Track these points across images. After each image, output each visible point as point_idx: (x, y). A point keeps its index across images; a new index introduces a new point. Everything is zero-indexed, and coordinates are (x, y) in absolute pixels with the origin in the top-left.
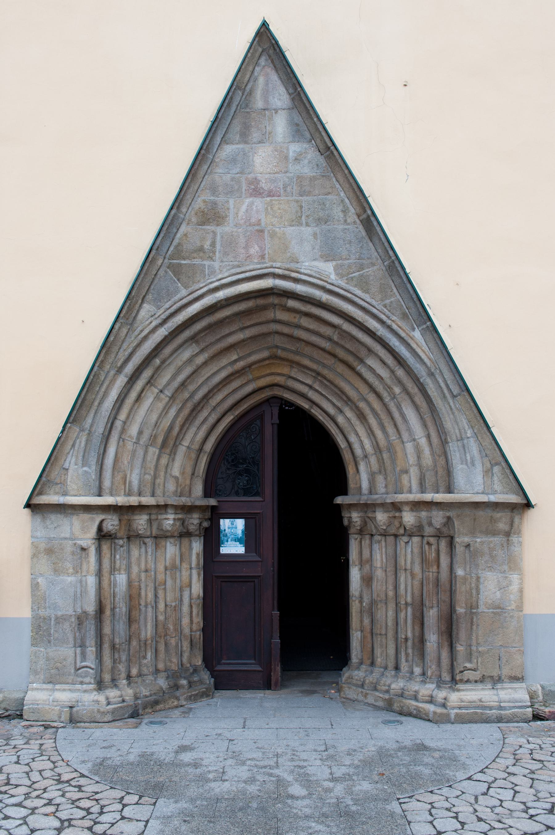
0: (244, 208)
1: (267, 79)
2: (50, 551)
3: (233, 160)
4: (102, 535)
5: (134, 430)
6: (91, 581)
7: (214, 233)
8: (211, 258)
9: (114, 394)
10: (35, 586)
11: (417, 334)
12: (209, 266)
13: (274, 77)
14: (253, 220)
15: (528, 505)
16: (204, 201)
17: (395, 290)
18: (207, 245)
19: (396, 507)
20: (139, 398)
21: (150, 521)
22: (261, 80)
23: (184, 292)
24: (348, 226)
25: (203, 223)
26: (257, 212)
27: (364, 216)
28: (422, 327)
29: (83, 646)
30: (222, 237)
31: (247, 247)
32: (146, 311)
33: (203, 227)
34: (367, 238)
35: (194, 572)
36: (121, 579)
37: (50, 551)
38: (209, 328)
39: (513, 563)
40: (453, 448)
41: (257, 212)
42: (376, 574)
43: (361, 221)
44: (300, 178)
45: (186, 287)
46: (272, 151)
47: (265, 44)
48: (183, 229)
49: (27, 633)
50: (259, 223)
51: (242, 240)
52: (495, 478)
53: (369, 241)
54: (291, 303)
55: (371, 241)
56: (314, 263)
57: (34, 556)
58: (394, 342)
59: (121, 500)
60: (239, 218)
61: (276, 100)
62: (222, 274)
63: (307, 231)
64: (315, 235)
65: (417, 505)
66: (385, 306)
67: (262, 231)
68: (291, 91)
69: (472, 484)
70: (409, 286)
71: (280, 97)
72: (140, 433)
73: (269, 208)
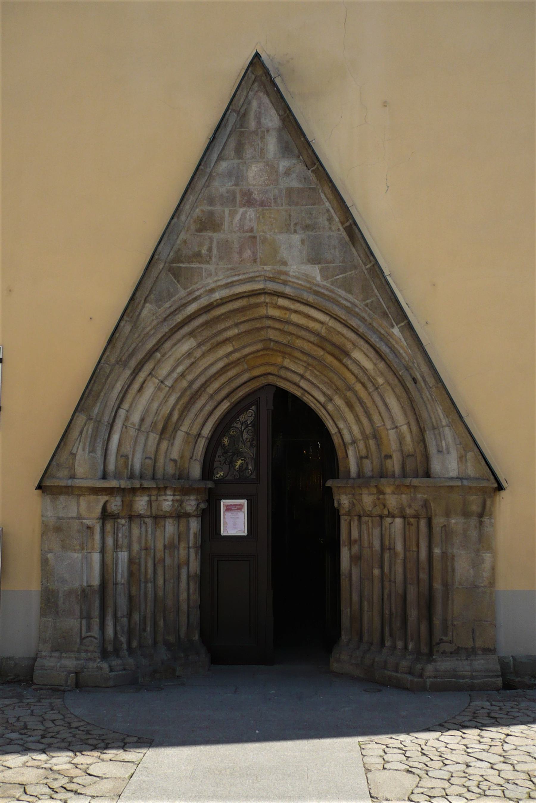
0: (238, 217)
2: (58, 529)
3: (230, 174)
4: (106, 515)
5: (136, 418)
6: (96, 557)
7: (211, 239)
8: (208, 262)
9: (119, 386)
10: (44, 562)
11: (396, 331)
12: (206, 269)
13: (266, 100)
14: (246, 228)
15: (500, 488)
16: (202, 211)
17: (376, 291)
18: (204, 251)
20: (141, 389)
21: (150, 502)
22: (255, 104)
23: (182, 293)
25: (199, 230)
26: (250, 220)
27: (348, 224)
28: (400, 325)
29: (89, 618)
30: (218, 243)
31: (240, 253)
33: (201, 234)
34: (350, 243)
35: (192, 551)
36: (123, 556)
37: (58, 529)
38: (206, 324)
40: (429, 436)
41: (250, 220)
43: (344, 228)
44: (290, 191)
45: (185, 289)
48: (183, 236)
50: (251, 230)
51: (236, 246)
52: (469, 464)
53: (352, 246)
54: (282, 302)
55: (354, 246)
57: (43, 534)
58: (374, 339)
59: (123, 484)
60: (234, 226)
61: (267, 120)
63: (296, 238)
64: (303, 241)
66: (367, 305)
67: (255, 237)
68: (281, 112)
70: (387, 287)
71: (272, 120)
72: (142, 420)
73: (261, 217)
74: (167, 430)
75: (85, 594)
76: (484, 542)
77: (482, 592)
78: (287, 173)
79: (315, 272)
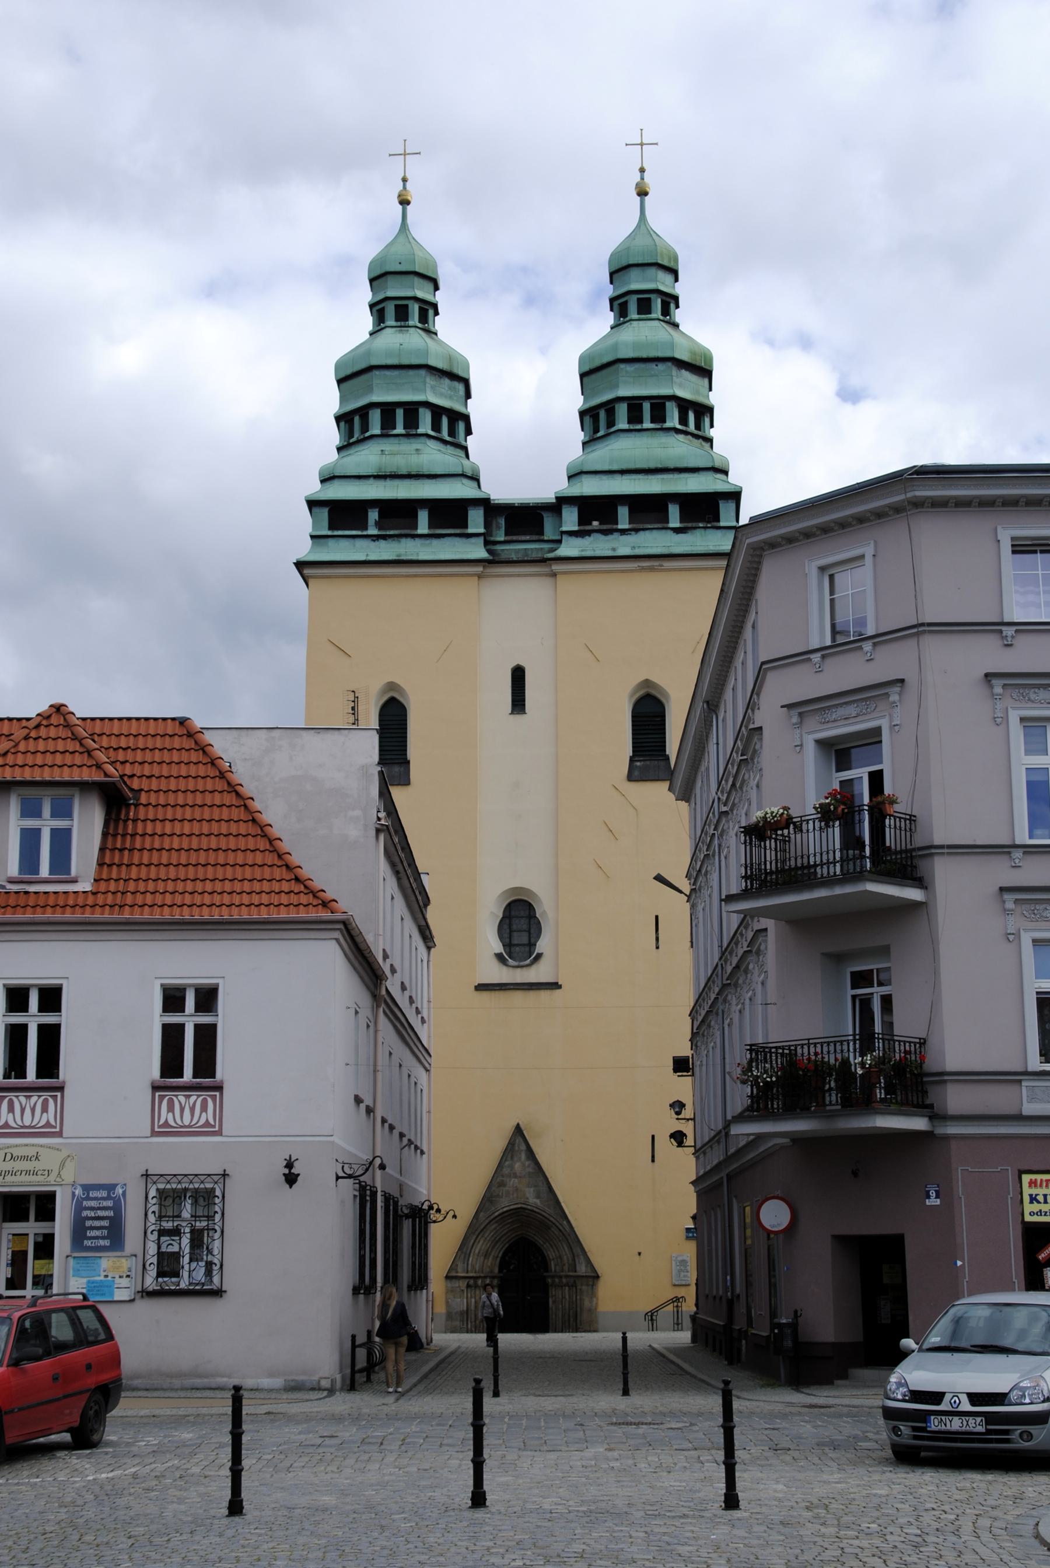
1: (519, 1140)
4: (468, 1286)
10: (447, 1302)
15: (598, 1277)
19: (560, 1277)
24: (544, 1188)
32: (482, 1214)
42: (558, 1300)
47: (518, 1130)
49: (444, 1318)
57: (447, 1293)
62: (504, 1204)
63: (532, 1190)
65: (567, 1276)
69: (582, 1269)
71: (523, 1147)
74: (486, 1255)
75: (462, 1313)
76: (593, 1294)
77: (592, 1311)
78: (529, 1166)
79: (538, 1201)
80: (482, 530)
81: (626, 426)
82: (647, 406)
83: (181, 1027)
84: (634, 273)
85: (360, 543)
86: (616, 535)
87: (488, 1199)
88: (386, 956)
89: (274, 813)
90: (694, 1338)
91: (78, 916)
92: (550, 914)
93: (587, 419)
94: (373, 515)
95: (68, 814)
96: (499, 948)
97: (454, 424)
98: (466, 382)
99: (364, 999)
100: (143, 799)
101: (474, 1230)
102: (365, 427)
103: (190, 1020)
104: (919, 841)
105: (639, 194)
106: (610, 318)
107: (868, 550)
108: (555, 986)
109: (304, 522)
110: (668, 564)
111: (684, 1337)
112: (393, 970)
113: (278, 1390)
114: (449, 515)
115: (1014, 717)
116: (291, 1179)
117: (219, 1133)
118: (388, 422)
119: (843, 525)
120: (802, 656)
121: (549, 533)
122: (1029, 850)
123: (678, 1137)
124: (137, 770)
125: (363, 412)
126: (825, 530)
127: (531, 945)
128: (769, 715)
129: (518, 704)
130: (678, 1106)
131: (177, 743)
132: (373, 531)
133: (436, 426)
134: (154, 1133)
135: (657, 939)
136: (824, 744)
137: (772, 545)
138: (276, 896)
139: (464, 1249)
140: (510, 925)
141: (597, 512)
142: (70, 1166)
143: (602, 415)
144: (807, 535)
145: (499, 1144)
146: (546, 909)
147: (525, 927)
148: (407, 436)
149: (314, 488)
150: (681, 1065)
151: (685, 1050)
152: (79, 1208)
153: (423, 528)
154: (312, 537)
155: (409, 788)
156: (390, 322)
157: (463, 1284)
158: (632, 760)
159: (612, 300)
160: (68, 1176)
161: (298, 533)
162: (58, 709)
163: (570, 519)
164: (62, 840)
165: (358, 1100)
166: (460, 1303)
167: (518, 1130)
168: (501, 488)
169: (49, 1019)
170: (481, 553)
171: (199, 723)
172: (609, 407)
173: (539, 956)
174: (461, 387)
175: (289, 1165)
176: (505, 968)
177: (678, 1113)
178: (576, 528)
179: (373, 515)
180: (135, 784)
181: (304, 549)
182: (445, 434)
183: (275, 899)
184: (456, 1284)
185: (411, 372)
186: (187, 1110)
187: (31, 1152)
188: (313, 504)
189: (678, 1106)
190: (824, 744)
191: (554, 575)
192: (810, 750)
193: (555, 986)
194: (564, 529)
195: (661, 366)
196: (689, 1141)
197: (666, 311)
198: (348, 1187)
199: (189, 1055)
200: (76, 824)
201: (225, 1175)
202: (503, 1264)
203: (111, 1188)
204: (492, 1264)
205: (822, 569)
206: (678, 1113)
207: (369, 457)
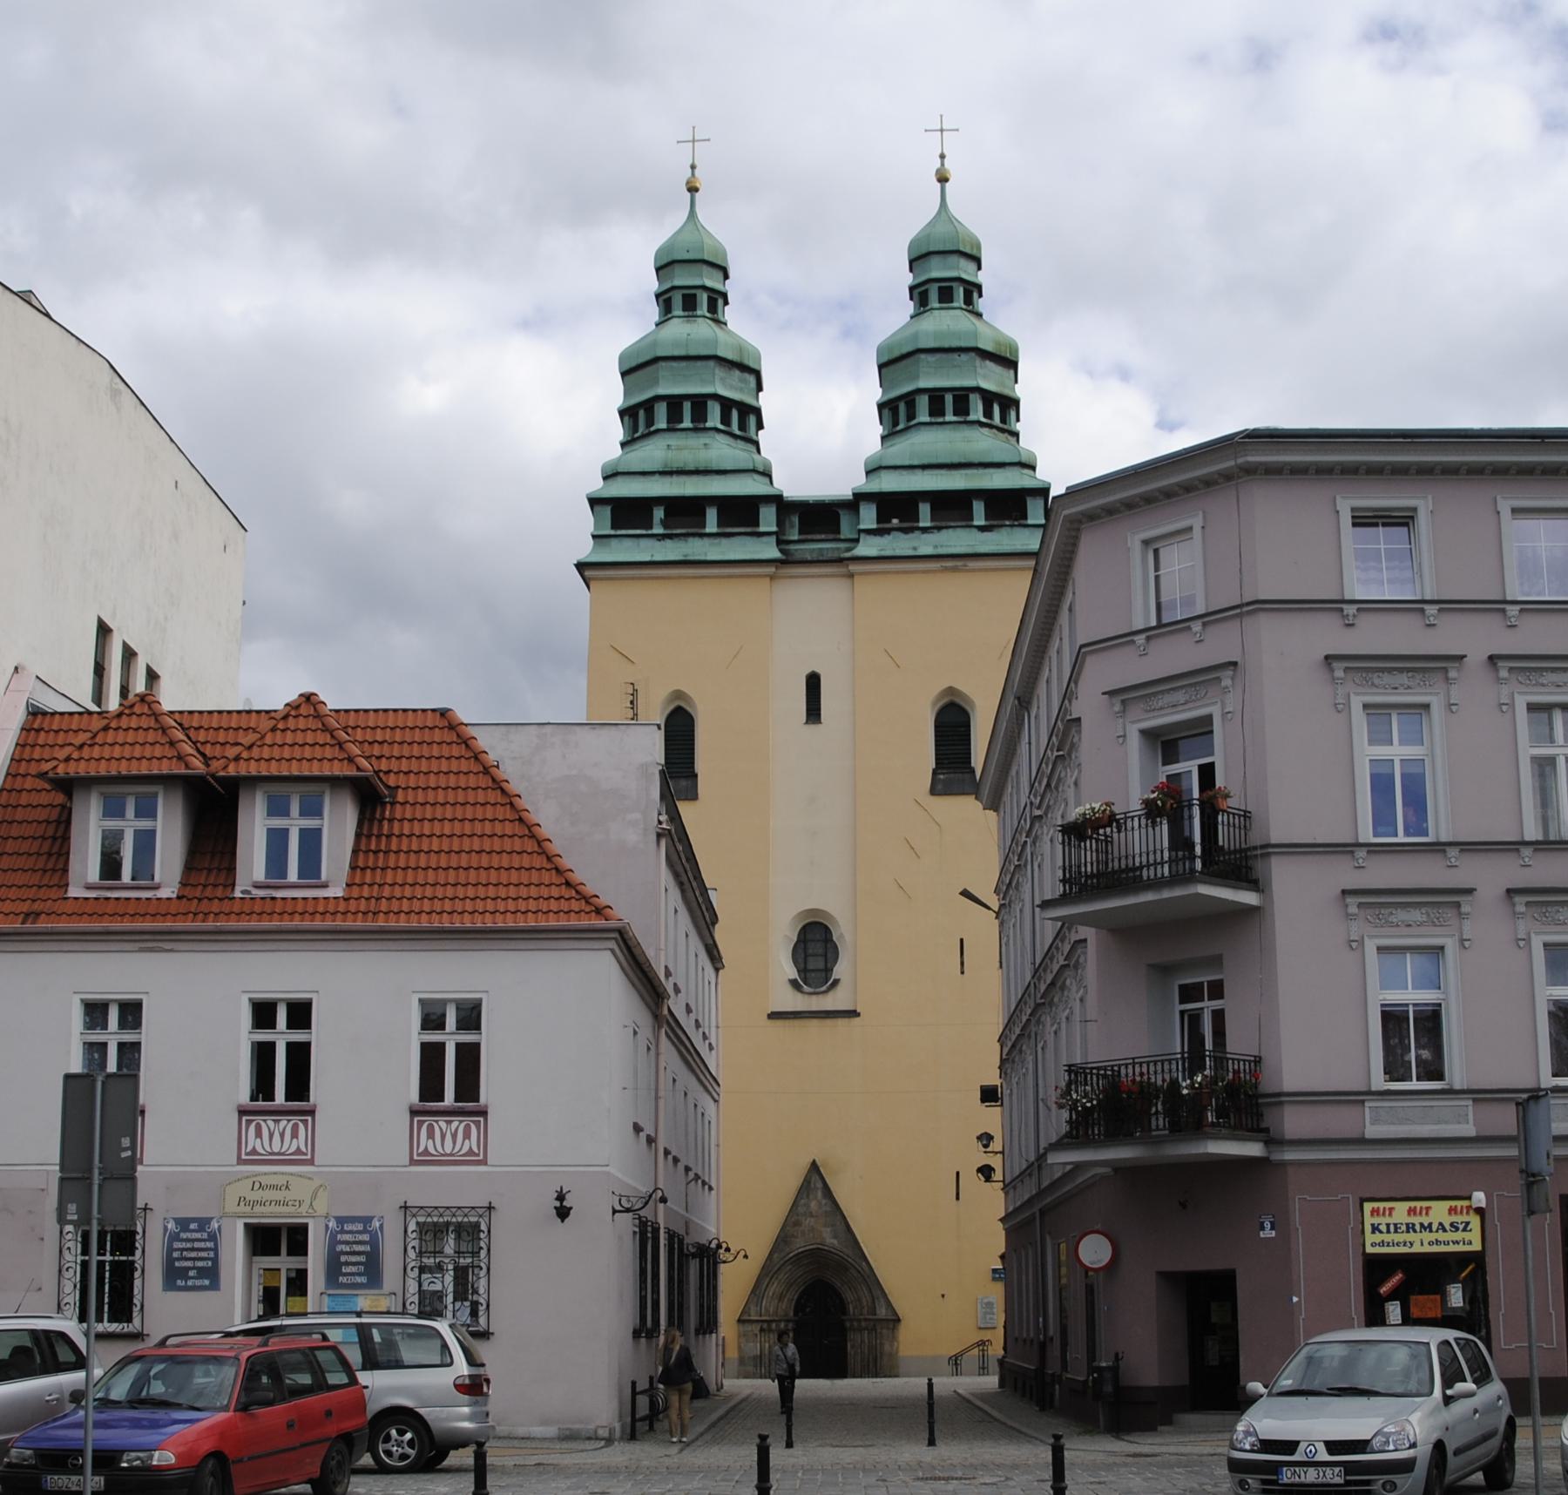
1: (815, 1178)
4: (762, 1330)
15: (899, 1320)
39: (894, 1338)
42: (856, 1344)
46: (816, 1203)
47: (814, 1167)
56: (830, 1240)
62: (800, 1245)
69: (882, 1312)
71: (820, 1185)
75: (755, 1358)
77: (893, 1356)
80: (774, 529)
81: (927, 419)
82: (949, 398)
83: (441, 1047)
84: (935, 260)
85: (644, 542)
86: (917, 533)
87: (783, 1239)
88: (668, 974)
89: (547, 816)
90: (1002, 1383)
91: (328, 924)
92: (848, 937)
93: (886, 412)
94: (659, 513)
95: (317, 812)
96: (793, 973)
97: (744, 418)
98: (757, 374)
99: (644, 1019)
100: (400, 797)
101: (768, 1271)
102: (650, 421)
103: (451, 1039)
104: (1255, 839)
105: (940, 180)
106: (910, 307)
107: (1197, 522)
108: (854, 1014)
109: (586, 522)
110: (972, 564)
111: (991, 1381)
112: (677, 990)
113: (551, 1440)
114: (740, 513)
115: (1357, 703)
116: (563, 1213)
117: (484, 1162)
118: (674, 415)
119: (1168, 494)
120: (1125, 639)
121: (846, 531)
122: (1374, 849)
123: (986, 1172)
124: (394, 765)
125: (648, 405)
126: (1149, 500)
127: (828, 971)
128: (1088, 704)
129: (814, 712)
130: (985, 1139)
131: (437, 736)
132: (658, 530)
133: (726, 420)
134: (413, 1162)
135: (962, 964)
136: (1148, 734)
137: (1091, 517)
138: (539, 900)
139: (757, 1291)
140: (805, 949)
141: (896, 510)
142: (323, 1197)
143: (902, 407)
144: (1130, 505)
145: (794, 1182)
146: (843, 932)
147: (821, 951)
148: (695, 430)
149: (596, 485)
150: (989, 1095)
151: (993, 1079)
152: (333, 1242)
153: (711, 526)
154: (594, 537)
155: (697, 803)
156: (677, 311)
157: (756, 1328)
158: (935, 773)
159: (912, 289)
160: (321, 1206)
161: (578, 532)
162: (308, 698)
163: (868, 516)
164: (311, 841)
165: (637, 1129)
166: (754, 1348)
167: (814, 1167)
168: (793, 483)
169: (298, 1036)
170: (773, 553)
171: (464, 715)
172: (910, 399)
173: (836, 982)
174: (752, 379)
175: (561, 1197)
176: (799, 995)
177: (986, 1146)
178: (874, 526)
179: (659, 513)
180: (392, 781)
181: (585, 549)
182: (735, 428)
183: (544, 906)
184: (749, 1327)
185: (699, 363)
186: (449, 1135)
187: (281, 1181)
188: (594, 502)
189: (985, 1139)
190: (1148, 734)
191: (851, 576)
192: (1134, 740)
193: (854, 1014)
194: (862, 527)
195: (964, 357)
196: (998, 1175)
197: (968, 300)
198: (626, 1222)
199: (450, 1075)
200: (326, 824)
201: (490, 1208)
202: (799, 1308)
203: (367, 1220)
204: (787, 1307)
205: (1146, 543)
206: (986, 1146)
207: (654, 452)
